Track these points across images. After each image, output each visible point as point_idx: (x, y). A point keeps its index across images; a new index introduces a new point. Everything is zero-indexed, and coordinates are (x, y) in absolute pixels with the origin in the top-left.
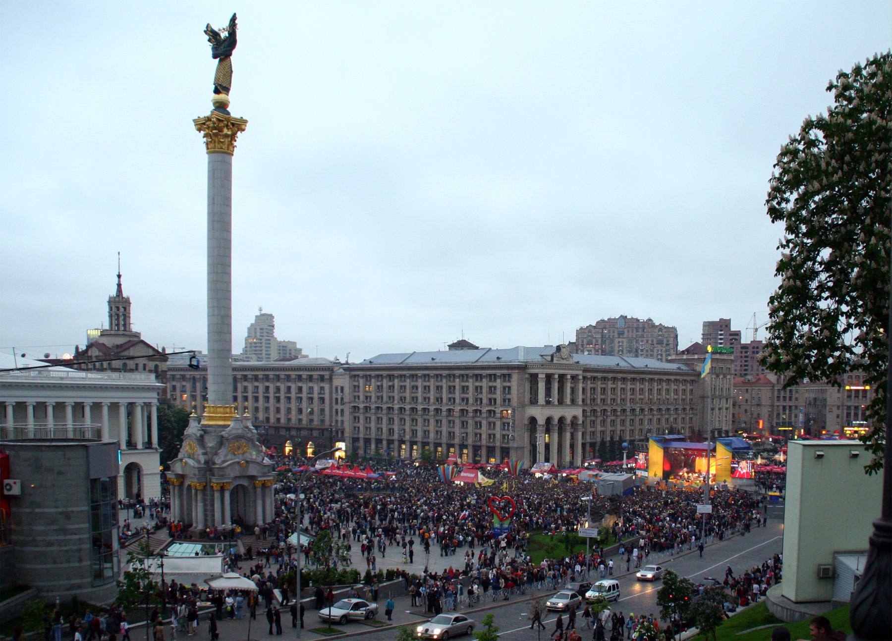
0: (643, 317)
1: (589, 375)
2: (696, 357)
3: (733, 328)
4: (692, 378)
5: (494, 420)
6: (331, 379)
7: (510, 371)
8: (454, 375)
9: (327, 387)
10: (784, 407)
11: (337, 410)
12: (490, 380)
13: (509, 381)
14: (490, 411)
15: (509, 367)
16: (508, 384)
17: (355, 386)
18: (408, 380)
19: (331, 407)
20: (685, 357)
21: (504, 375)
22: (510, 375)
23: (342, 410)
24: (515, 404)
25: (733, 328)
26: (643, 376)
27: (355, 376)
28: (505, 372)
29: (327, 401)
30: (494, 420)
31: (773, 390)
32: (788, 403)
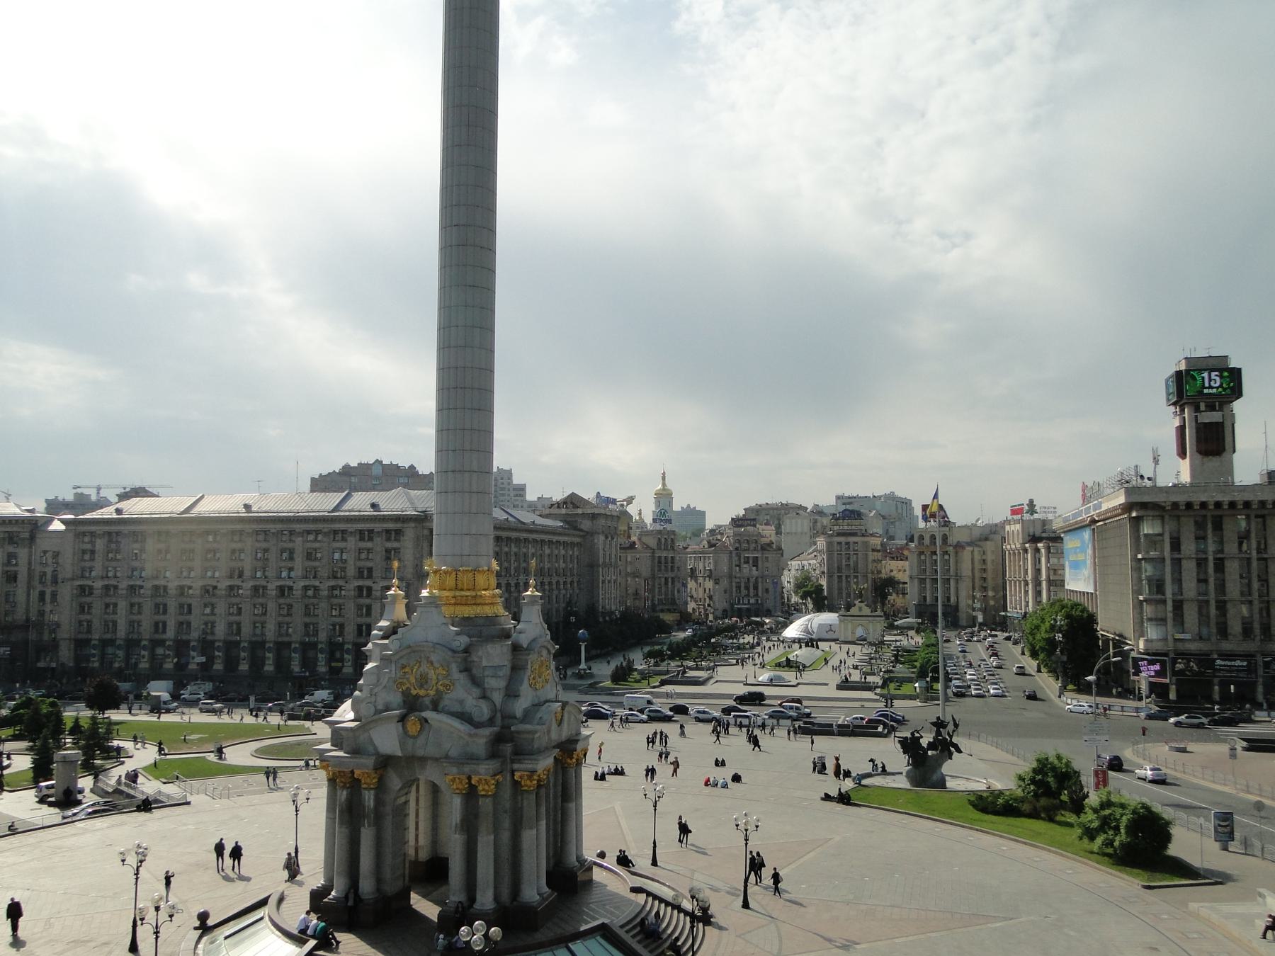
0: (404, 463)
1: (504, 534)
2: (580, 511)
3: (516, 480)
4: (578, 540)
5: (368, 601)
6: (32, 538)
7: (399, 525)
8: (292, 532)
9: (22, 553)
10: (666, 579)
11: (42, 594)
12: (362, 539)
13: (397, 540)
14: (360, 588)
15: (397, 519)
16: (395, 545)
17: (84, 552)
18: (299, 540)
19: (30, 586)
20: (563, 511)
21: (388, 531)
22: (398, 532)
23: (54, 595)
24: (409, 576)
25: (516, 480)
26: (534, 536)
27: (84, 534)
28: (391, 526)
29: (23, 576)
30: (368, 601)
31: (653, 557)
32: (670, 575)
